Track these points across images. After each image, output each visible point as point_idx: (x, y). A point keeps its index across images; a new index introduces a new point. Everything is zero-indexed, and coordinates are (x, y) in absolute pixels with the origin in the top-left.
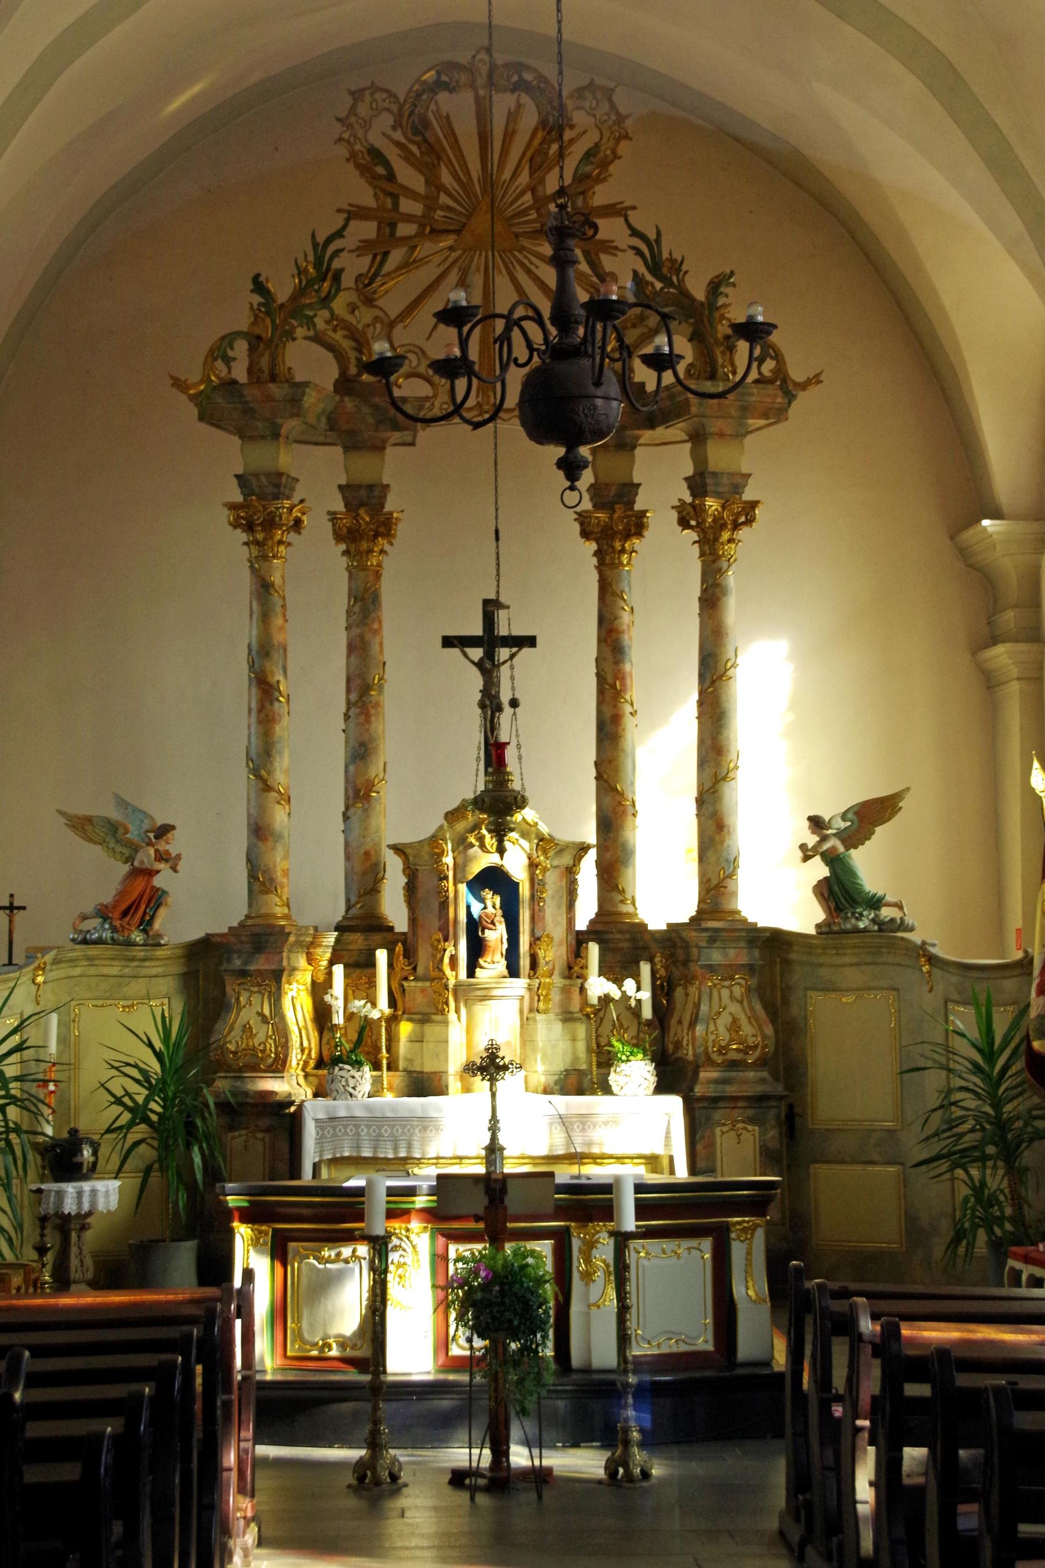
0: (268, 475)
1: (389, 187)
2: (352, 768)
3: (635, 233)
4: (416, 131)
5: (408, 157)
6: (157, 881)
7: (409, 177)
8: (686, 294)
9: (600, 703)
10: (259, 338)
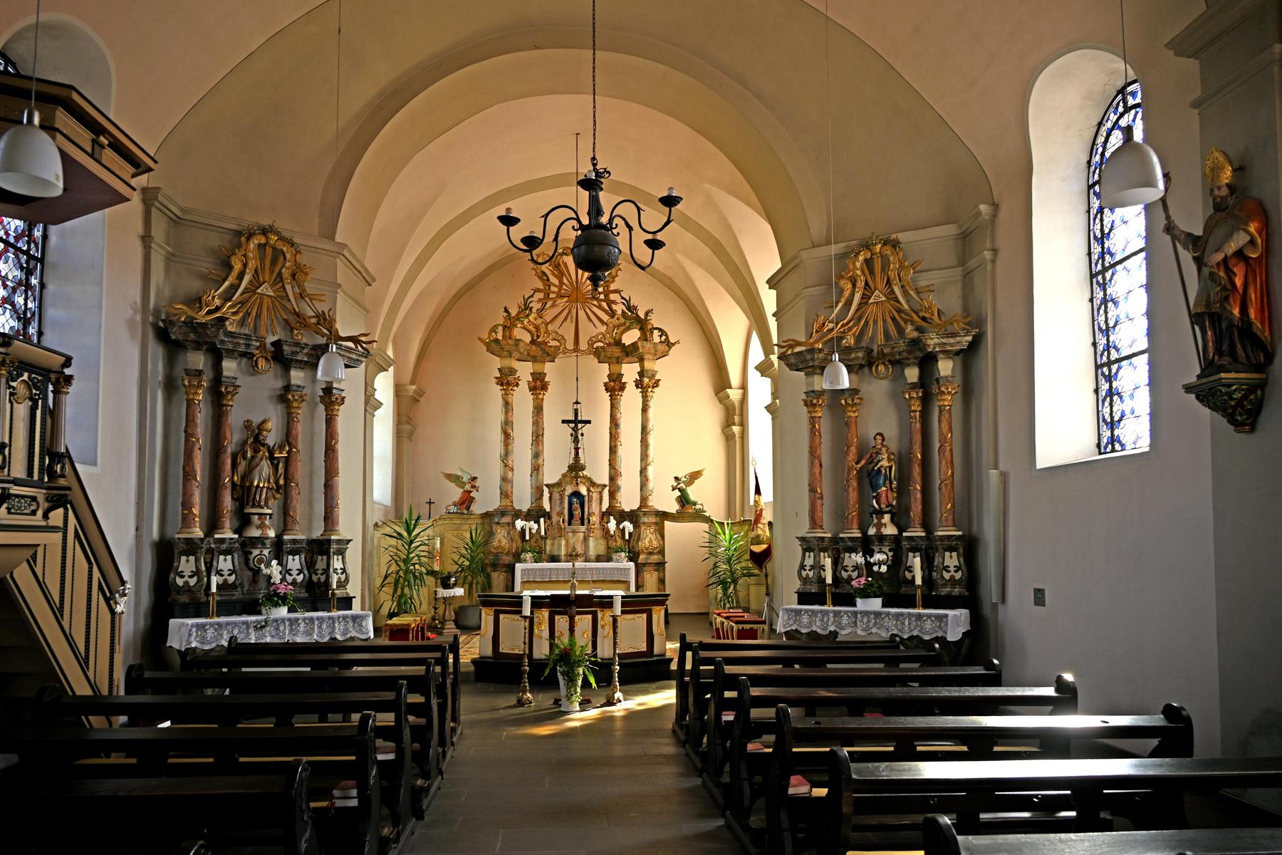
0: (508, 368)
1: (548, 283)
2: (533, 461)
3: (623, 298)
4: (556, 266)
5: (554, 274)
6: (472, 494)
7: (554, 280)
8: (638, 316)
9: (610, 441)
10: (506, 326)
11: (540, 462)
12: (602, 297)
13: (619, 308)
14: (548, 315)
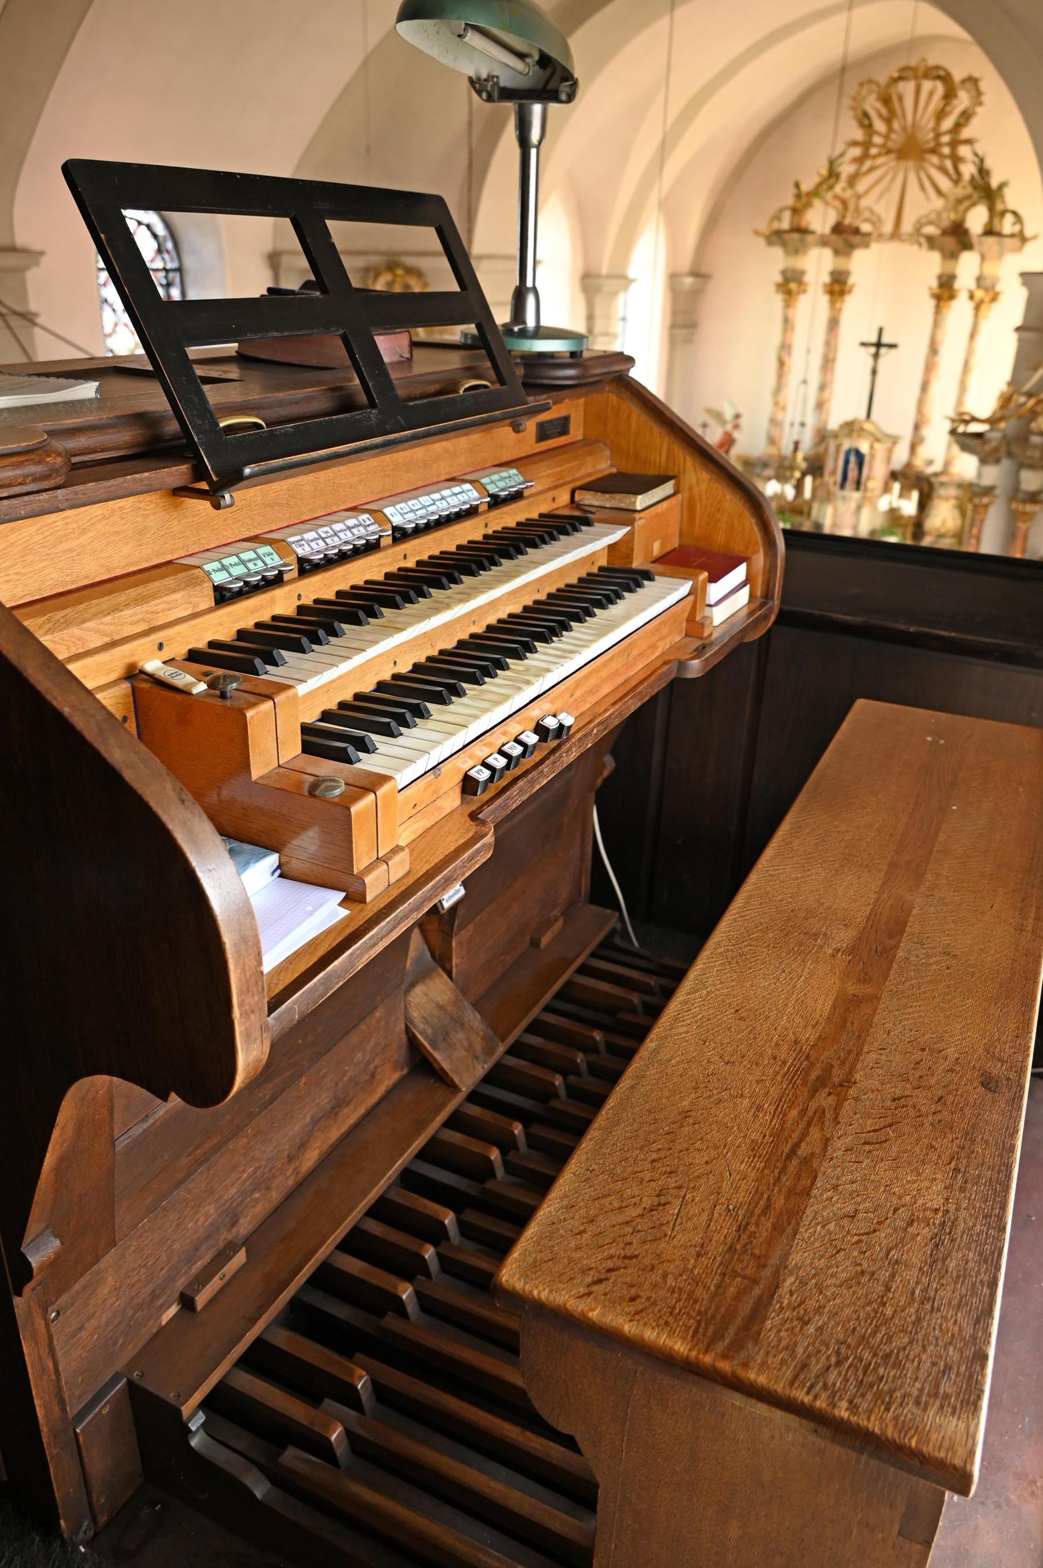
5: (880, 115)
7: (879, 126)
11: (826, 394)
12: (946, 150)
13: (968, 170)
14: (862, 186)
